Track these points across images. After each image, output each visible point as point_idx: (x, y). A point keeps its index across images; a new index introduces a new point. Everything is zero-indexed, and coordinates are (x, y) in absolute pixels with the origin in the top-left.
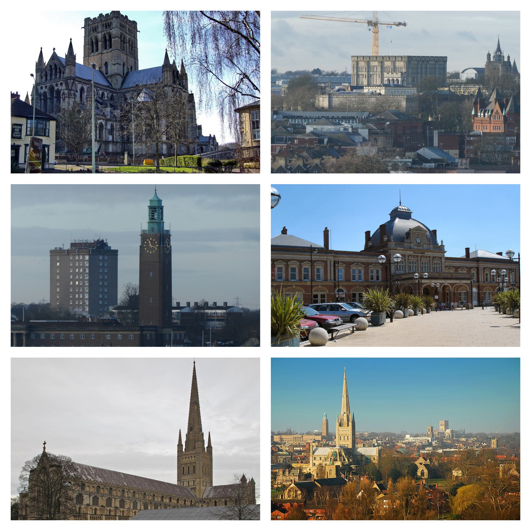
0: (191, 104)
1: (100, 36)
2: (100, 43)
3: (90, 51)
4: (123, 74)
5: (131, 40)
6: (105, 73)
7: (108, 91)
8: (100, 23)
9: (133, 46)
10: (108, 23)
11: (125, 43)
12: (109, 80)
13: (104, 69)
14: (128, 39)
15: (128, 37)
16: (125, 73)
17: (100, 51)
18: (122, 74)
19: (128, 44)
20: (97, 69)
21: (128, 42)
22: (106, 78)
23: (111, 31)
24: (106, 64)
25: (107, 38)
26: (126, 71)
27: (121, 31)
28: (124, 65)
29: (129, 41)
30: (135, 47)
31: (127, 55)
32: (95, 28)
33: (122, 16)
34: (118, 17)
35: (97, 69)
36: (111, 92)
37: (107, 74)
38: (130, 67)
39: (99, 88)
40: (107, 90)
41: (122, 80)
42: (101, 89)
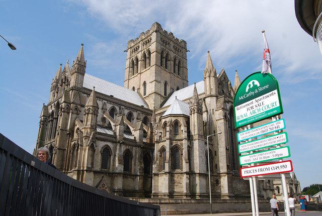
1: (140, 56)
2: (139, 63)
4: (165, 94)
6: (142, 93)
8: (141, 42)
9: (181, 65)
11: (168, 60)
12: (147, 101)
13: (142, 91)
15: (172, 55)
16: (168, 94)
17: (139, 72)
18: (163, 94)
19: (172, 63)
21: (173, 59)
22: (143, 99)
23: (150, 47)
24: (145, 84)
25: (147, 56)
28: (166, 84)
29: (175, 60)
33: (166, 32)
36: (143, 113)
37: (145, 94)
38: (176, 88)
40: (137, 110)
41: (162, 101)
42: (127, 108)
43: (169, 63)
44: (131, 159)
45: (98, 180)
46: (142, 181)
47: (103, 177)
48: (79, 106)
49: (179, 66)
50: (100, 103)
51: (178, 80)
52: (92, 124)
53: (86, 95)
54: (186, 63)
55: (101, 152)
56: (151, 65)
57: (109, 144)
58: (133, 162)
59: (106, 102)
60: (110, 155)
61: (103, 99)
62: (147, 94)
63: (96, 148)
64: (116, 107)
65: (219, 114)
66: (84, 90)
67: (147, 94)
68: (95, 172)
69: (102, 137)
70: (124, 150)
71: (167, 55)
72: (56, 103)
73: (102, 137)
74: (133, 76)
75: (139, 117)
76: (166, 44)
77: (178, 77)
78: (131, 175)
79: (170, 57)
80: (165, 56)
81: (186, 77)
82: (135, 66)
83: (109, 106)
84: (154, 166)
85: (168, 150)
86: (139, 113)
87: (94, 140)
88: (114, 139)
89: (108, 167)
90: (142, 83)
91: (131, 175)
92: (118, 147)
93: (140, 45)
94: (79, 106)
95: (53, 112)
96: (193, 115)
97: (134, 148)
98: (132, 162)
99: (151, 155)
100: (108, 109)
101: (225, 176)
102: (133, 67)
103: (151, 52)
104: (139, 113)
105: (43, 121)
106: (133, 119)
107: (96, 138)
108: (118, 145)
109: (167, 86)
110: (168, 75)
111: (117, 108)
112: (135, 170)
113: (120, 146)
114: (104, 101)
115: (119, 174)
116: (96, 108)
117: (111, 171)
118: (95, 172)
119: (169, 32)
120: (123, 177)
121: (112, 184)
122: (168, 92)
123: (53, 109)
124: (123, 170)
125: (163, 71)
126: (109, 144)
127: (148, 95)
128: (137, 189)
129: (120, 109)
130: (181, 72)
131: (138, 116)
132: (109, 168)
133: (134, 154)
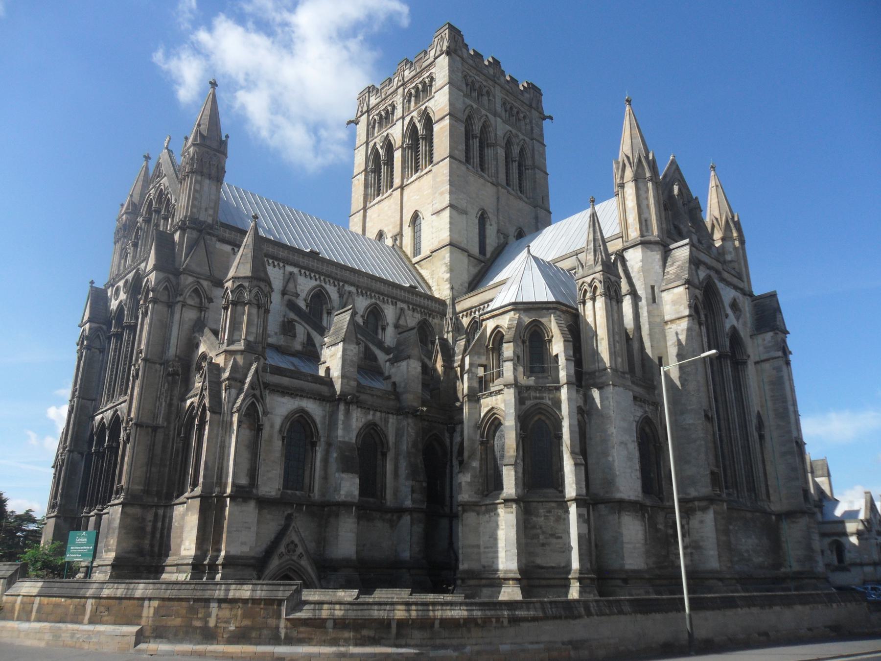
0: (769, 335)
2: (398, 155)
3: (371, 191)
5: (514, 140)
7: (405, 306)
8: (400, 90)
9: (529, 162)
10: (423, 83)
11: (488, 145)
14: (500, 133)
15: (500, 128)
16: (489, 249)
17: (397, 182)
18: (475, 250)
19: (501, 152)
20: (389, 242)
26: (492, 242)
27: (468, 101)
30: (534, 167)
31: (496, 184)
32: (387, 112)
34: (455, 51)
35: (389, 242)
36: (415, 307)
38: (512, 231)
39: (352, 284)
40: (395, 300)
43: (489, 152)
44: (384, 455)
45: (272, 527)
46: (418, 529)
47: (289, 518)
48: (205, 284)
49: (520, 166)
50: (275, 274)
51: (518, 208)
52: (251, 338)
53: (228, 248)
54: (543, 155)
55: (280, 431)
56: (435, 160)
57: (313, 408)
58: (389, 467)
59: (296, 270)
60: (314, 445)
61: (287, 262)
62: (425, 251)
63: (265, 421)
64: (327, 287)
65: (674, 303)
66: (221, 232)
67: (425, 251)
68: (263, 503)
69: (285, 381)
70: (360, 425)
71: (485, 127)
72: (130, 276)
73: (285, 381)
74: (377, 199)
75: (402, 322)
76: (480, 94)
77: (520, 198)
78: (382, 510)
79: (492, 135)
80: (477, 129)
81: (545, 197)
82: (384, 169)
83: (305, 285)
84: (465, 479)
85: (509, 422)
86: (402, 309)
87: (257, 392)
88: (324, 389)
89: (307, 481)
90: (407, 217)
91: (382, 510)
92: (341, 416)
93: (398, 99)
94: (205, 284)
95: (120, 308)
96: (589, 304)
97: (392, 419)
98: (384, 466)
99: (448, 440)
100: (303, 295)
101: (704, 509)
102: (377, 171)
103: (434, 119)
104: (402, 309)
105: (87, 338)
106: (384, 329)
107: (267, 386)
108: (342, 407)
109: (488, 226)
110: (490, 190)
111: (333, 292)
112: (396, 492)
113: (347, 413)
114: (289, 269)
115: (346, 505)
116: (262, 285)
117: (316, 495)
118: (263, 503)
119: (487, 60)
120: (359, 518)
121: (322, 541)
122: (492, 242)
123: (123, 296)
124: (357, 493)
125: (472, 178)
126: (313, 408)
127: (428, 253)
128: (406, 555)
129: (341, 296)
130: (527, 184)
131: (399, 318)
132: (311, 489)
133: (391, 439)
